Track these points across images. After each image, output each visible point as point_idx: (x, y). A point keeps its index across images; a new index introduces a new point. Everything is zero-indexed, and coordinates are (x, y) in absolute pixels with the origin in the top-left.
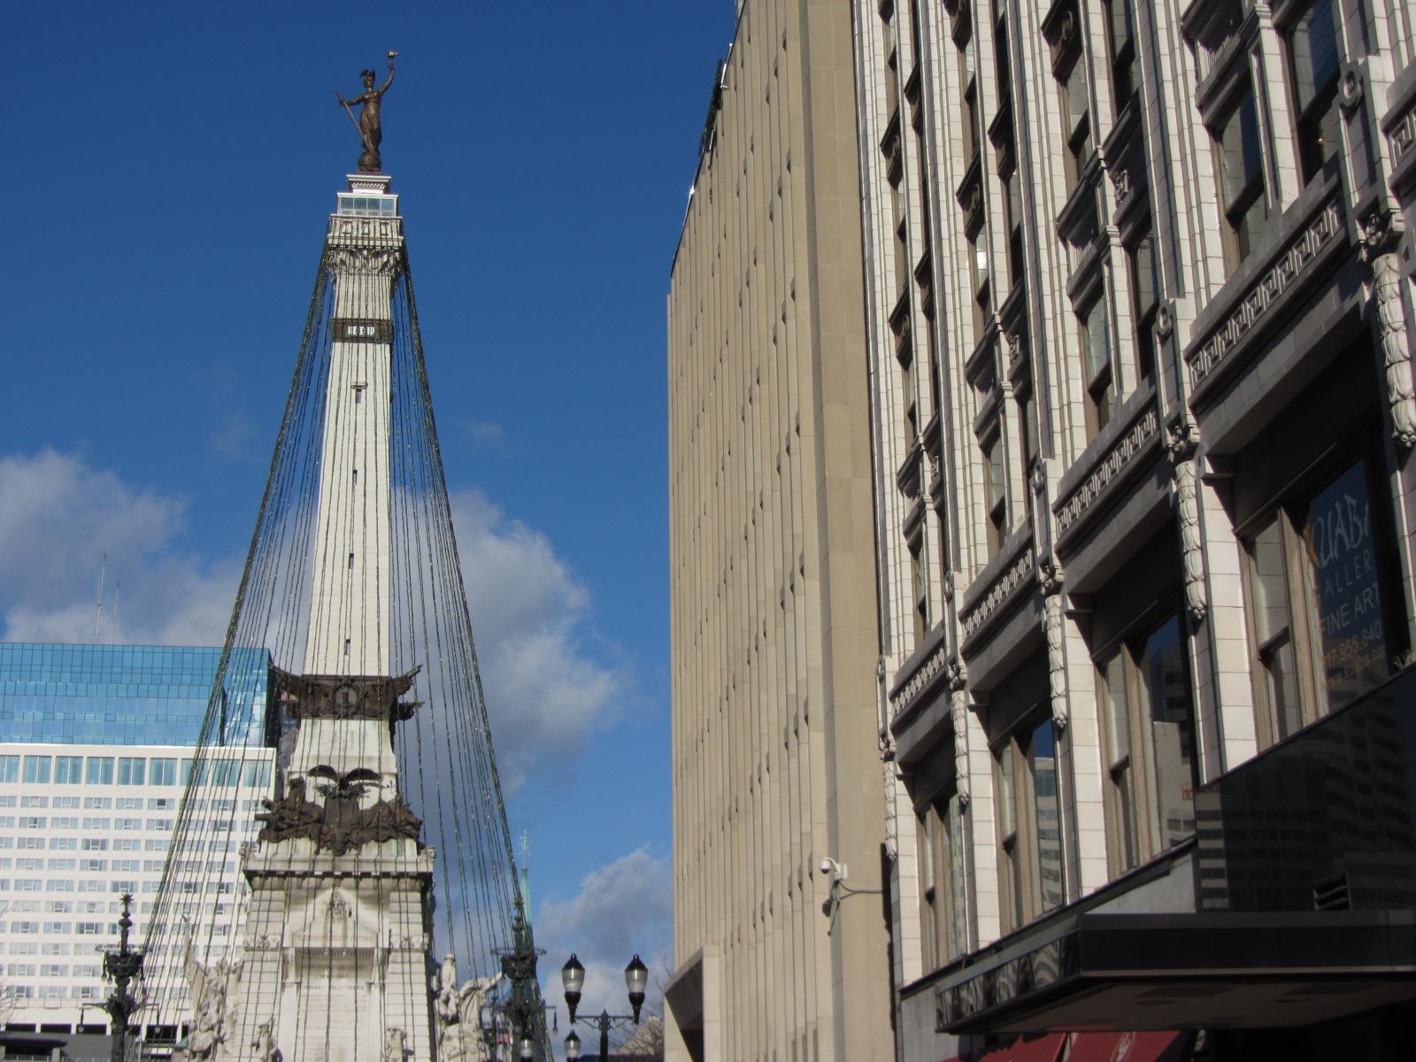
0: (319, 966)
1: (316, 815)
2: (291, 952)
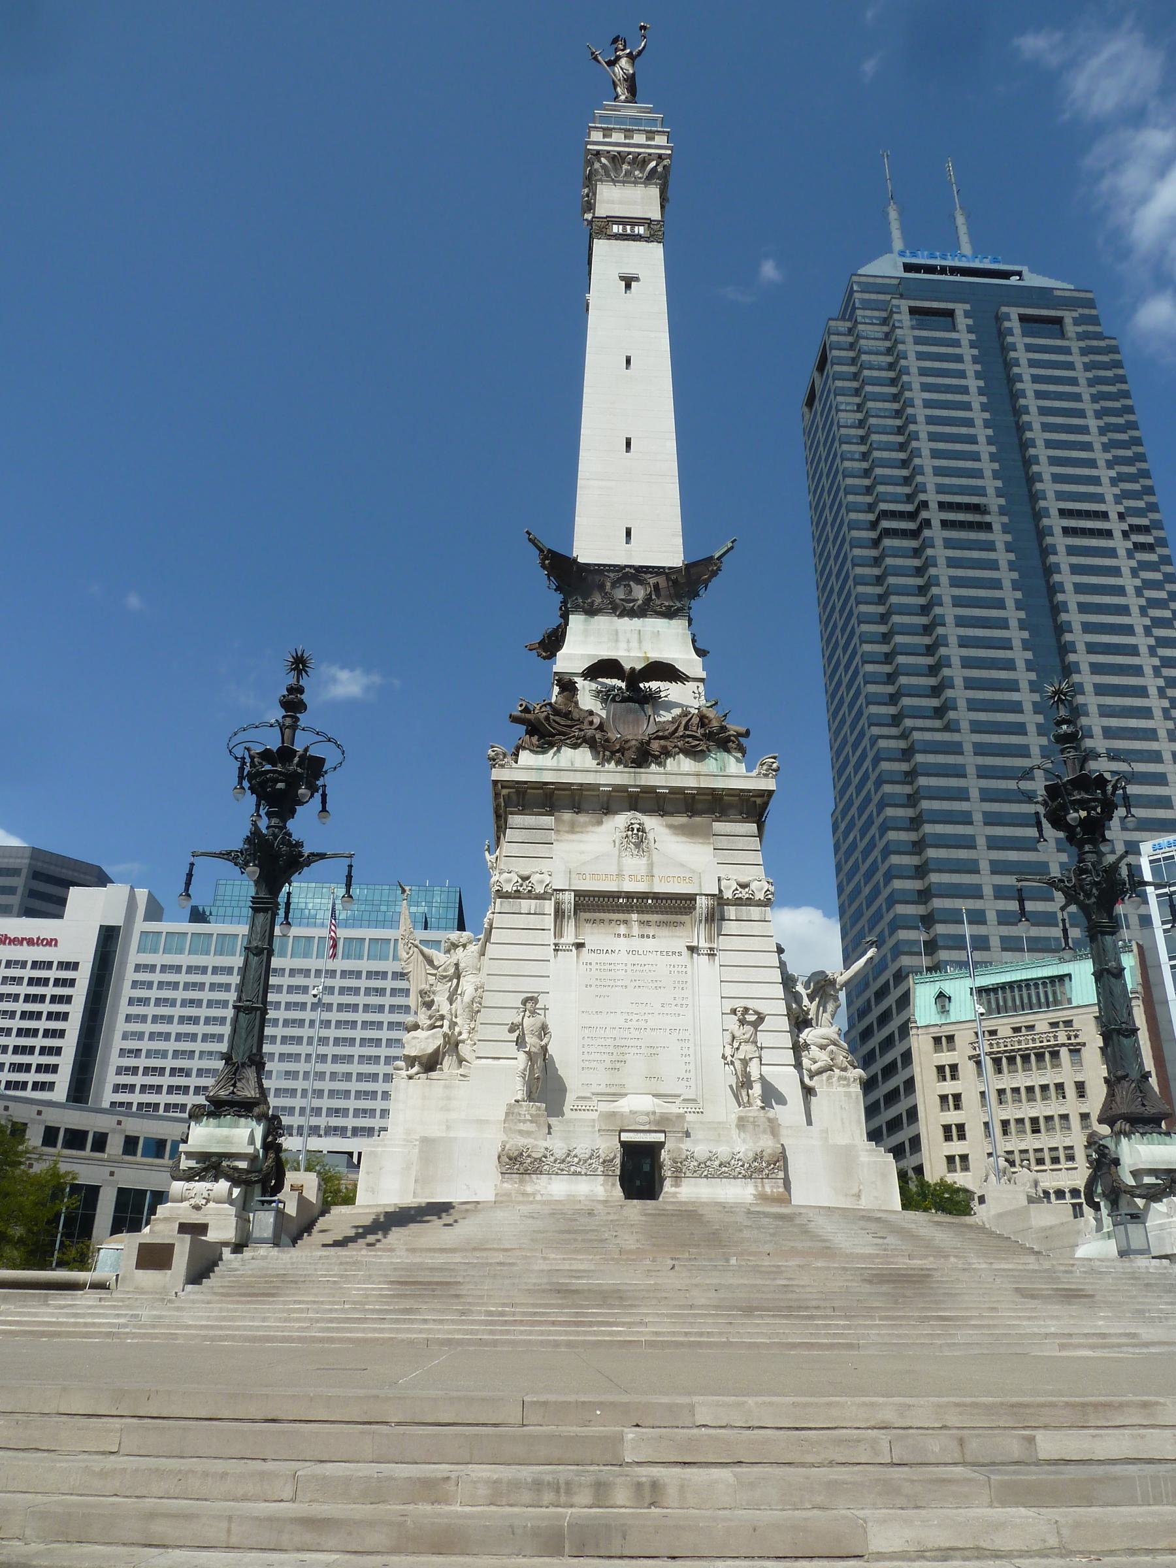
0: (611, 921)
1: (597, 721)
2: (568, 899)
